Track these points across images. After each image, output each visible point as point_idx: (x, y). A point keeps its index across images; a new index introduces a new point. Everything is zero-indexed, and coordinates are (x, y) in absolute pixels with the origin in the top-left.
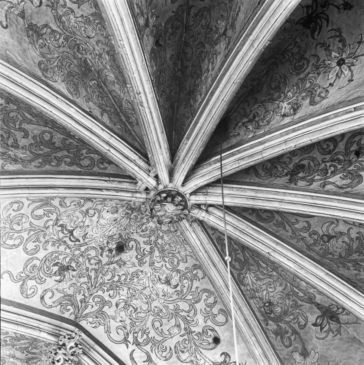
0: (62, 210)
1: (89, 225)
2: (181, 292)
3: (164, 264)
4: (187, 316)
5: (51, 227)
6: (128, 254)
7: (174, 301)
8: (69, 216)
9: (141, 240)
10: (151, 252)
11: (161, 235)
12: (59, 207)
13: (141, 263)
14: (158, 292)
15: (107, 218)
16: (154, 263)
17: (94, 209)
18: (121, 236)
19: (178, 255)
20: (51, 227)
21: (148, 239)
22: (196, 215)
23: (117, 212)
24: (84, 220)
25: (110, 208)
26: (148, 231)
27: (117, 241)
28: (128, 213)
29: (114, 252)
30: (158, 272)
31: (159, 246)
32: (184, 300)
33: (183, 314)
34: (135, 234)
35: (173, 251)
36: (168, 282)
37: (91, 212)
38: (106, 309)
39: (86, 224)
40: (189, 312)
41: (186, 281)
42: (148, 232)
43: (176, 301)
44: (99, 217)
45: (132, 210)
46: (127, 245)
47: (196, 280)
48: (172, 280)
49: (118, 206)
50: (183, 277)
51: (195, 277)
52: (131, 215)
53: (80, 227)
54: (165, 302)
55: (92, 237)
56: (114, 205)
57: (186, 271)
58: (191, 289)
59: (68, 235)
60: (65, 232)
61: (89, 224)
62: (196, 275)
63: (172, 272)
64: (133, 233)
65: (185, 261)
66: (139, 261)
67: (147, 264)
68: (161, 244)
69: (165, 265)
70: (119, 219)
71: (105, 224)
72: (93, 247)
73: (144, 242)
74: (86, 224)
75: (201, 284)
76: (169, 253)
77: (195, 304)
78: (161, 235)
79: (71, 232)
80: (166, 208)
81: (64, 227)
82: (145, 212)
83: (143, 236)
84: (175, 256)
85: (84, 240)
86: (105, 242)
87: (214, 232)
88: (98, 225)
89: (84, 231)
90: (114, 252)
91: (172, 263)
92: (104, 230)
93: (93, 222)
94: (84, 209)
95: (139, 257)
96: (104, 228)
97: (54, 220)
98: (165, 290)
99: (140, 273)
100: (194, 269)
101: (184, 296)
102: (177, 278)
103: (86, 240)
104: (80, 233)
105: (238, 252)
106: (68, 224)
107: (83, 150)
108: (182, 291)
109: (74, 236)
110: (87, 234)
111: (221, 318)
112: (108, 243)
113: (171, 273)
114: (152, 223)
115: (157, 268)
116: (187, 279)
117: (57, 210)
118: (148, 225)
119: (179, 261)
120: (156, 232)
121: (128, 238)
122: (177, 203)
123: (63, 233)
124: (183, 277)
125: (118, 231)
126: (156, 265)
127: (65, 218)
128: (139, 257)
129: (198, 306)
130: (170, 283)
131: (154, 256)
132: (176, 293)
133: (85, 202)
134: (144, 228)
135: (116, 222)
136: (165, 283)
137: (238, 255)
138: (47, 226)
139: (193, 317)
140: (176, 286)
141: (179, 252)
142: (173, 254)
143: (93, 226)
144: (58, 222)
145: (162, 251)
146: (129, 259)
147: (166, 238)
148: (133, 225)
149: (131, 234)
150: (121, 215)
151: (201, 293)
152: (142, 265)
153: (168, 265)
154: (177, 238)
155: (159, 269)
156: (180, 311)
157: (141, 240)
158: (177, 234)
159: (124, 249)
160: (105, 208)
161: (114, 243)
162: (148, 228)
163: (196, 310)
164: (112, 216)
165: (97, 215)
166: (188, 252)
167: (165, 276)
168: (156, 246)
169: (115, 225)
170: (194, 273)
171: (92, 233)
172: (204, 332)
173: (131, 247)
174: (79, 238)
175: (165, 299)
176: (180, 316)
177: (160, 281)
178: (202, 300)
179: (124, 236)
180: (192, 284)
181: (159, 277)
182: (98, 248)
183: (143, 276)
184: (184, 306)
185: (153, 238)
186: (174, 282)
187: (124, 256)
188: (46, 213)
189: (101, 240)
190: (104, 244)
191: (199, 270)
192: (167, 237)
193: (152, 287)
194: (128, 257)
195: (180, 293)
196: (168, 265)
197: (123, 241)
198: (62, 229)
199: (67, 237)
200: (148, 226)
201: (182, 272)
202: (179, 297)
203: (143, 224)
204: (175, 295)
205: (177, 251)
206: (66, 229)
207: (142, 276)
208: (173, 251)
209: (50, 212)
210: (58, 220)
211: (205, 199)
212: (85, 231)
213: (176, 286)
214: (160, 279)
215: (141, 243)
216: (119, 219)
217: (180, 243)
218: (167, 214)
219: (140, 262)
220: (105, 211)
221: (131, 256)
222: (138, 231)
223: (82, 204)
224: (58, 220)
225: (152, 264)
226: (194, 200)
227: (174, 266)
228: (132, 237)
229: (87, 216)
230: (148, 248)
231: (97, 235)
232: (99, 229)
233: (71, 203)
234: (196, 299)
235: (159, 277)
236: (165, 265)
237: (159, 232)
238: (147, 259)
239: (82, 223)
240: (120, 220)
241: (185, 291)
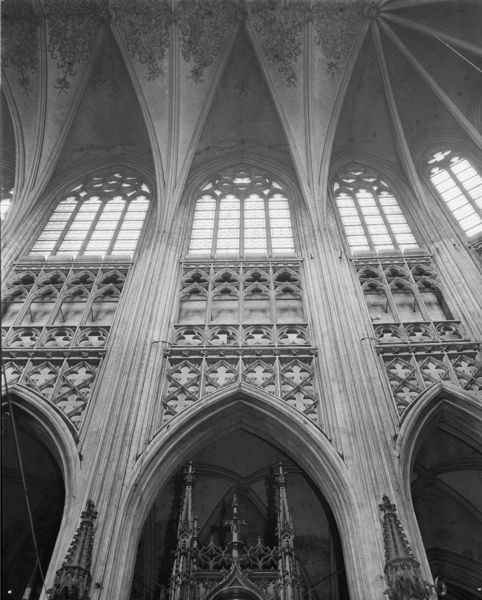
18: (345, 7)
36: (342, 31)
38: (322, 19)
111: (345, 54)
129: (343, 45)
140: (343, 35)
172: (338, 52)
184: (339, 41)
186: (343, 33)
187: (339, 13)
213: (343, 35)
225: (343, 23)
226: (379, 18)
230: (347, 18)
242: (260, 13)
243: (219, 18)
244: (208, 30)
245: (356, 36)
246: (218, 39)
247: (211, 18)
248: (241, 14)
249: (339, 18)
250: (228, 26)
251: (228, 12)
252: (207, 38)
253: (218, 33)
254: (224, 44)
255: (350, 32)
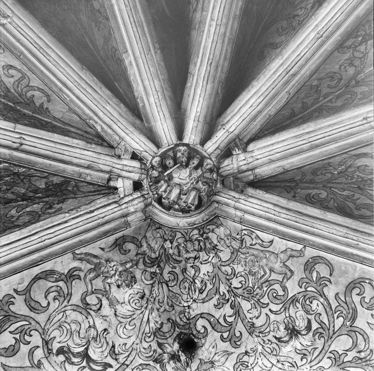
0: (42, 318)
1: (106, 327)
2: (322, 328)
3: (265, 311)
4: (358, 355)
5: (44, 361)
6: (207, 345)
7: (323, 351)
8: (60, 326)
9: (208, 307)
10: (238, 312)
11: (230, 271)
12: (32, 314)
13: (235, 342)
14: (291, 361)
15: (126, 300)
16: (253, 324)
17: (93, 293)
18: (174, 324)
19: (274, 276)
20: (44, 361)
21: (217, 296)
22: (232, 166)
23: (134, 280)
24: (92, 323)
25: (117, 277)
26: (208, 284)
27: (175, 335)
28: (154, 273)
29: (183, 358)
30: (269, 332)
31: (240, 291)
32: (336, 335)
33: (351, 355)
34: (194, 306)
35: (263, 276)
36: (293, 332)
37: (92, 300)
39: (100, 328)
40: (355, 345)
41: (315, 302)
42: (209, 286)
43: (326, 348)
44: (111, 304)
45: (155, 262)
46: (195, 332)
47: (327, 285)
48: (297, 324)
49: (128, 266)
50: (308, 302)
51: (322, 282)
52: (161, 274)
53: (95, 339)
54: (312, 364)
55: (127, 346)
56: (120, 269)
57: (303, 289)
58: (331, 307)
59: (84, 364)
60: (75, 360)
61: (105, 325)
62: (319, 278)
63: (287, 311)
64: (189, 307)
65: (289, 273)
66: (230, 340)
67: (245, 334)
68: (240, 285)
69: (270, 310)
70: (147, 293)
71: (131, 313)
72: (141, 365)
73: (215, 306)
74: (100, 328)
75: (337, 283)
76: (261, 288)
77: (355, 325)
78: (230, 271)
79: (85, 355)
80: (176, 180)
81: (66, 352)
82: (179, 256)
83: (207, 299)
84: (272, 282)
85: (116, 360)
86: (155, 346)
87: (295, 193)
88: (122, 320)
89: (105, 345)
90: (183, 358)
91: (275, 297)
92: (138, 325)
93: (108, 319)
94: (76, 299)
95: (225, 335)
96: (135, 321)
97: (41, 345)
98: (299, 347)
99: (246, 358)
100: (311, 272)
101: (332, 329)
102: (301, 313)
103: (121, 359)
104: (100, 350)
105: (355, 198)
106: (70, 343)
107: (10, 211)
108: (321, 323)
109: (94, 362)
110: (113, 346)
112: (160, 345)
113: (287, 315)
114: (203, 265)
115: (264, 327)
116: (315, 298)
117: (33, 323)
118: (201, 275)
119: (281, 283)
120: (220, 274)
121: (188, 319)
122: (184, 159)
123: (73, 363)
124: (308, 302)
125: (162, 316)
126: (258, 323)
127: (56, 333)
128: (225, 335)
129: (360, 323)
130: (297, 331)
131: (245, 312)
132: (317, 337)
133: (69, 284)
134: (198, 285)
135: (145, 299)
136: (291, 338)
137: (358, 201)
138: (36, 363)
139: (367, 346)
140: (309, 327)
141: (271, 270)
142: (267, 281)
143: (114, 328)
144: (50, 347)
145: (249, 294)
146: (213, 351)
147: (239, 269)
148: (179, 292)
149: (187, 310)
150: (147, 282)
151: (347, 299)
152: (239, 343)
153: (274, 308)
154: (251, 251)
155: (267, 325)
156: (342, 357)
157: (208, 307)
158: (248, 245)
159: (196, 343)
160: (109, 281)
161: (170, 341)
162: (205, 280)
163: (362, 332)
164: (131, 291)
165: (105, 302)
166: (282, 256)
167: (282, 328)
168: (236, 295)
169: (150, 307)
170: (314, 279)
171: (122, 341)
173: (202, 331)
174: (105, 361)
175: (309, 361)
176: (349, 364)
177: (282, 342)
178: (359, 307)
179: (178, 320)
180: (326, 299)
181: (275, 337)
182: (151, 363)
183: (253, 358)
185: (223, 289)
186: (301, 324)
187: (204, 353)
188: (17, 336)
189: (146, 345)
190: (155, 351)
191: (317, 267)
192: (240, 266)
193: (278, 361)
194: (211, 349)
195: (321, 330)
196: (274, 308)
197: (183, 331)
198: (66, 358)
199: (84, 367)
200: (202, 276)
201: (300, 295)
202: (326, 338)
203: (194, 280)
204: (317, 340)
205: (268, 271)
206: (73, 354)
207: (251, 360)
208: (263, 276)
209: (23, 332)
210: (47, 343)
211: (225, 130)
212: (107, 343)
213: (309, 327)
214: (279, 339)
215: (213, 311)
216: (147, 293)
217: (262, 255)
218: (185, 188)
219: (232, 342)
220: (114, 288)
221: (214, 344)
222: (195, 297)
223: (66, 292)
224: (47, 343)
225: (251, 328)
226: (211, 147)
227: (283, 299)
228: (193, 314)
229: (92, 313)
230: (227, 310)
231: (133, 339)
232: (127, 326)
233: (46, 297)
234: (350, 316)
235: (275, 337)
236: (270, 310)
237: (223, 269)
238: (240, 327)
239: (92, 330)
240: (151, 291)
241: (326, 321)
245: (310, 252)
249: (228, 354)
255: (293, 288)
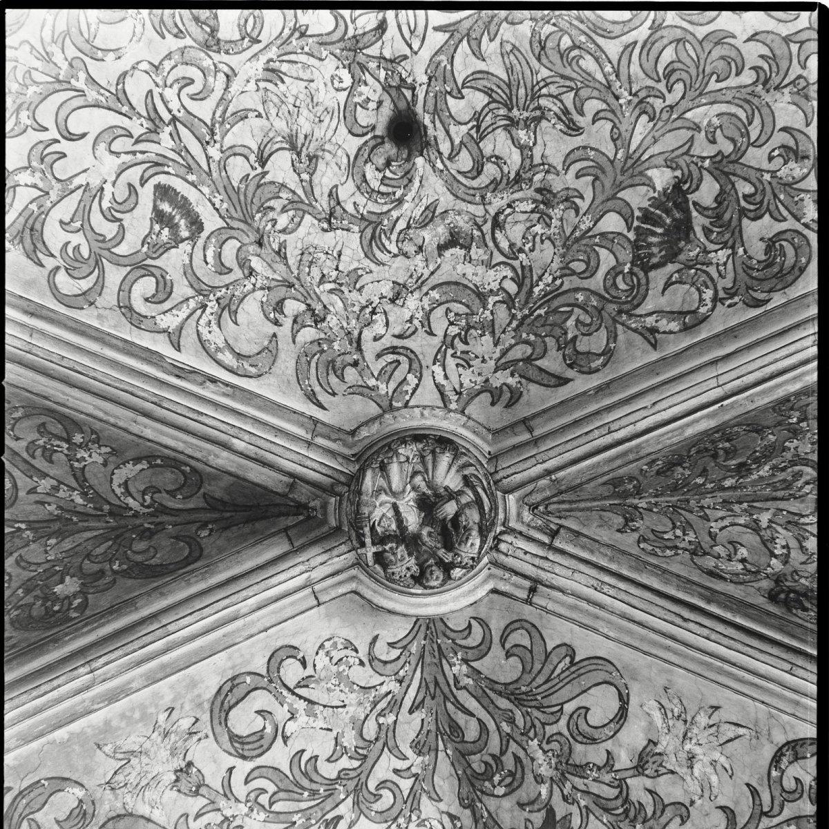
242: (410, 726)
243: (350, 242)
244: (230, 117)
246: (139, 223)
247: (353, 144)
248: (427, 505)
250: (270, 350)
251: (423, 345)
252: (137, 89)
253: (196, 224)
254: (87, 299)
